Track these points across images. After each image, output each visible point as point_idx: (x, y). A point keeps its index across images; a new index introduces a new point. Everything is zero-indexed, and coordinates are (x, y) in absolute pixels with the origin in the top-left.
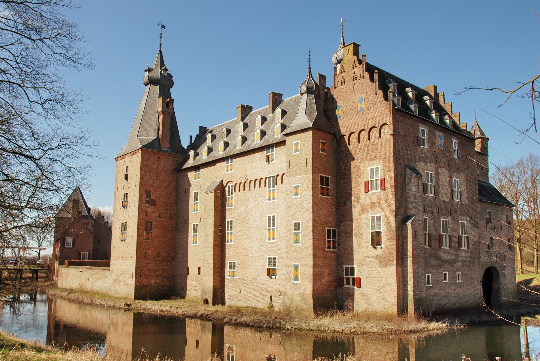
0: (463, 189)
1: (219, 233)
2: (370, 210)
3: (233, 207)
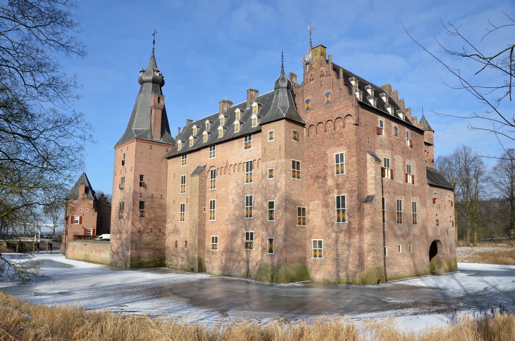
0: (414, 173)
1: (203, 212)
3: (216, 188)
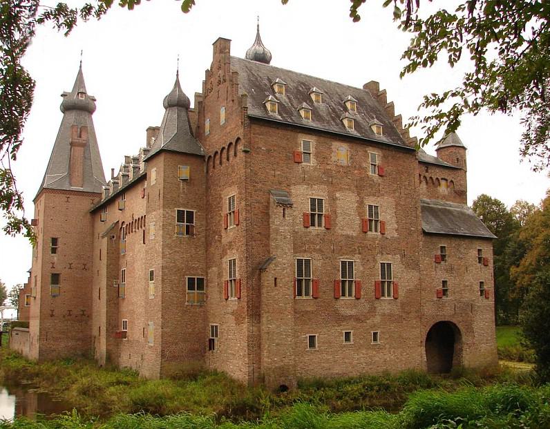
2: (228, 251)
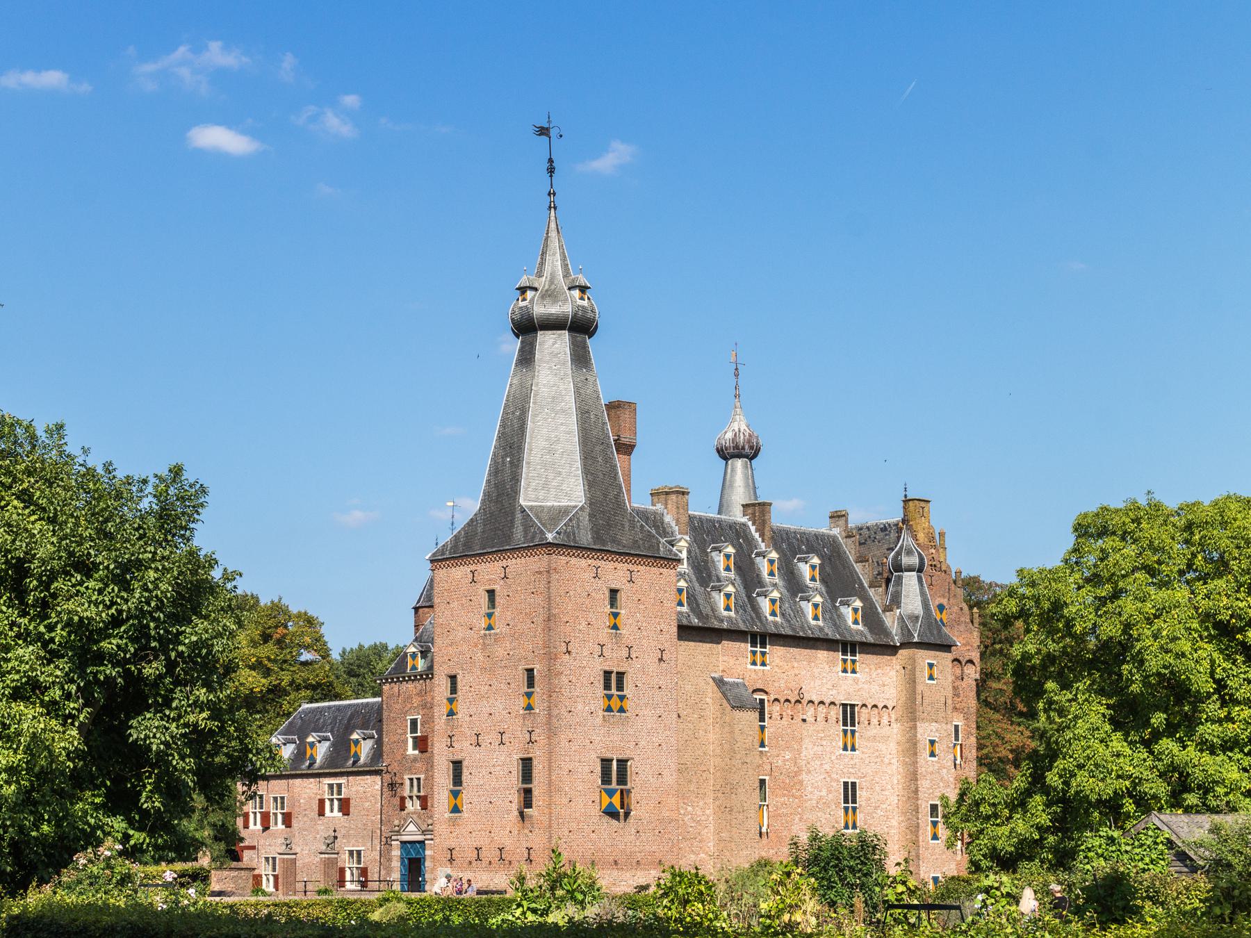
3: (766, 749)
